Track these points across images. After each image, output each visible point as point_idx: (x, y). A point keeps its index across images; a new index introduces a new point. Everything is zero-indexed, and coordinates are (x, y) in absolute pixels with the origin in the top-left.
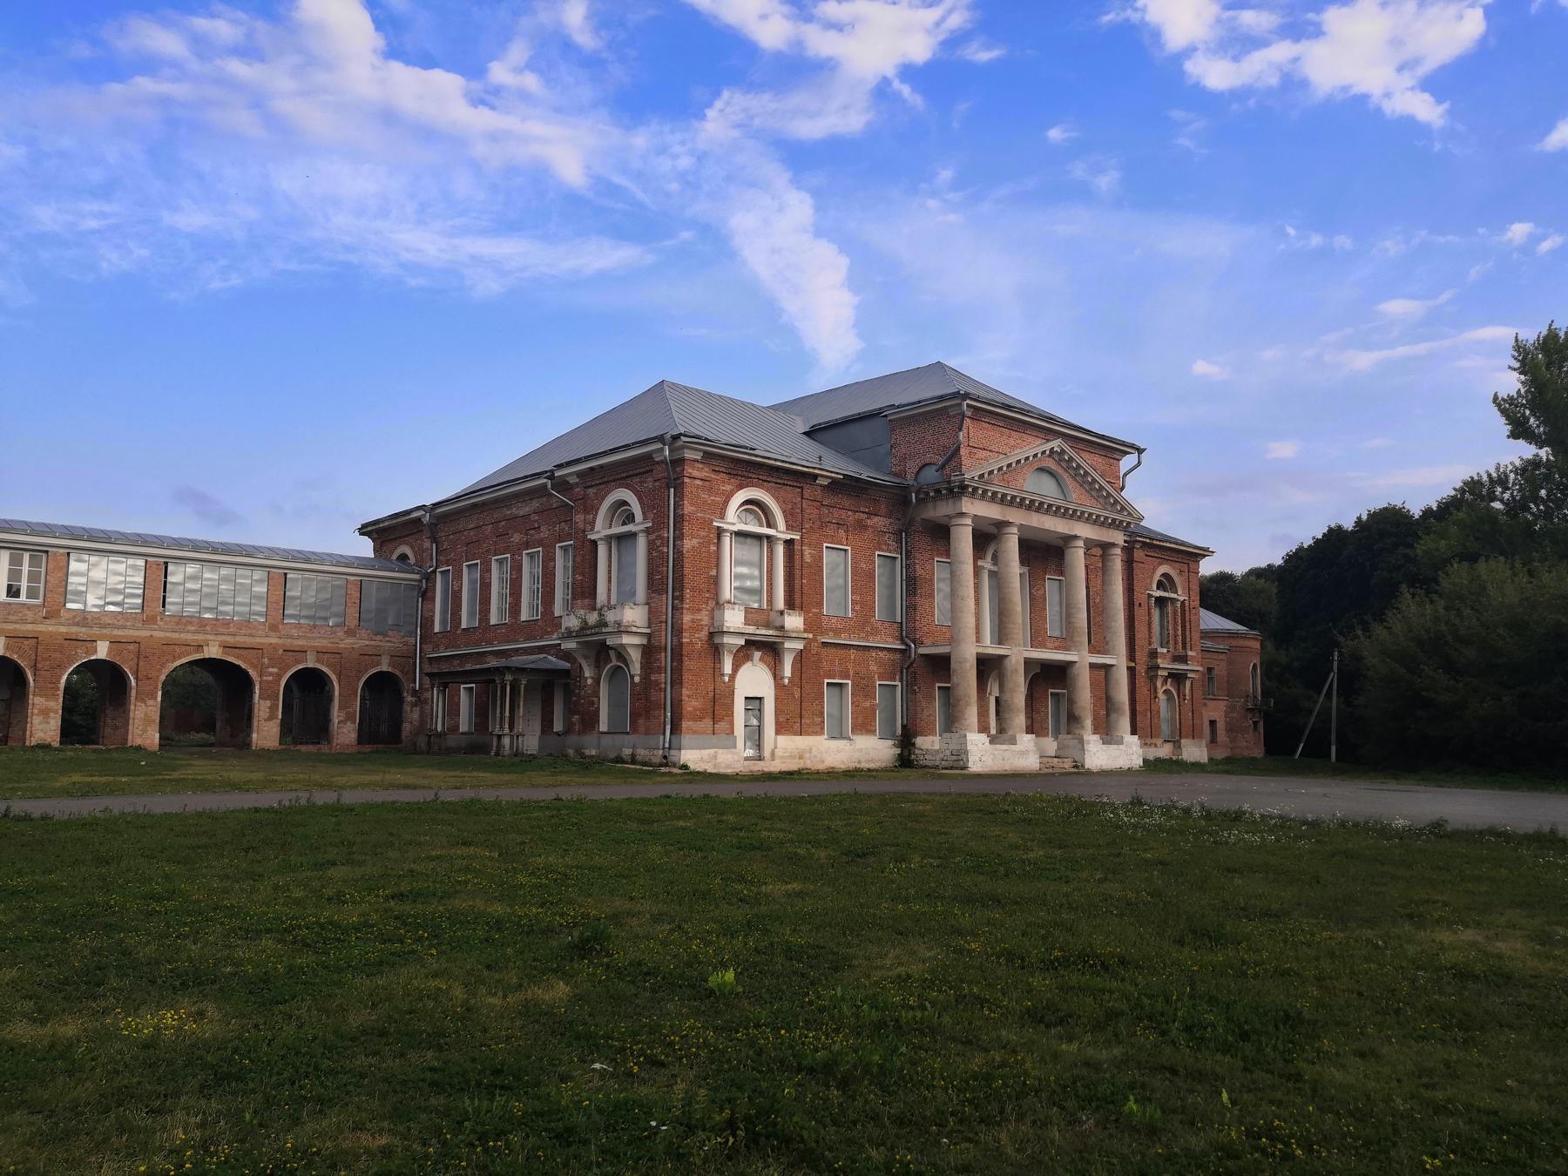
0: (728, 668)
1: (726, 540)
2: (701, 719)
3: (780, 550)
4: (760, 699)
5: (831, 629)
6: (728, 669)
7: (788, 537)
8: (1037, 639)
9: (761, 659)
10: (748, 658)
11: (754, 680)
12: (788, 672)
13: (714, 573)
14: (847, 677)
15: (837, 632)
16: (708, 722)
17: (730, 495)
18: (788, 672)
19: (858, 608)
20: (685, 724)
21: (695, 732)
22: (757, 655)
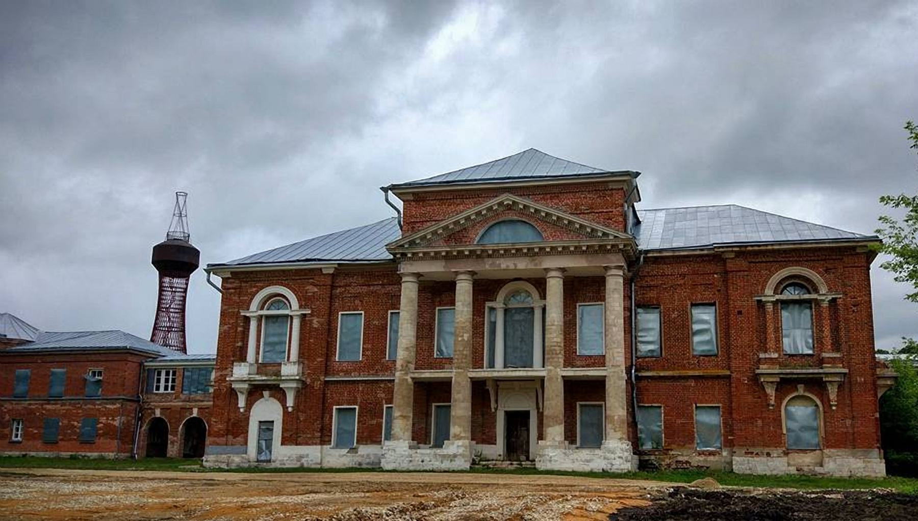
0: (242, 403)
2: (223, 436)
3: (296, 323)
4: (273, 422)
5: (342, 371)
6: (242, 403)
7: (299, 313)
8: (570, 360)
10: (262, 396)
11: (267, 410)
12: (290, 402)
13: (240, 344)
15: (347, 373)
16: (230, 437)
17: (253, 295)
18: (290, 402)
21: (218, 444)
22: (266, 393)
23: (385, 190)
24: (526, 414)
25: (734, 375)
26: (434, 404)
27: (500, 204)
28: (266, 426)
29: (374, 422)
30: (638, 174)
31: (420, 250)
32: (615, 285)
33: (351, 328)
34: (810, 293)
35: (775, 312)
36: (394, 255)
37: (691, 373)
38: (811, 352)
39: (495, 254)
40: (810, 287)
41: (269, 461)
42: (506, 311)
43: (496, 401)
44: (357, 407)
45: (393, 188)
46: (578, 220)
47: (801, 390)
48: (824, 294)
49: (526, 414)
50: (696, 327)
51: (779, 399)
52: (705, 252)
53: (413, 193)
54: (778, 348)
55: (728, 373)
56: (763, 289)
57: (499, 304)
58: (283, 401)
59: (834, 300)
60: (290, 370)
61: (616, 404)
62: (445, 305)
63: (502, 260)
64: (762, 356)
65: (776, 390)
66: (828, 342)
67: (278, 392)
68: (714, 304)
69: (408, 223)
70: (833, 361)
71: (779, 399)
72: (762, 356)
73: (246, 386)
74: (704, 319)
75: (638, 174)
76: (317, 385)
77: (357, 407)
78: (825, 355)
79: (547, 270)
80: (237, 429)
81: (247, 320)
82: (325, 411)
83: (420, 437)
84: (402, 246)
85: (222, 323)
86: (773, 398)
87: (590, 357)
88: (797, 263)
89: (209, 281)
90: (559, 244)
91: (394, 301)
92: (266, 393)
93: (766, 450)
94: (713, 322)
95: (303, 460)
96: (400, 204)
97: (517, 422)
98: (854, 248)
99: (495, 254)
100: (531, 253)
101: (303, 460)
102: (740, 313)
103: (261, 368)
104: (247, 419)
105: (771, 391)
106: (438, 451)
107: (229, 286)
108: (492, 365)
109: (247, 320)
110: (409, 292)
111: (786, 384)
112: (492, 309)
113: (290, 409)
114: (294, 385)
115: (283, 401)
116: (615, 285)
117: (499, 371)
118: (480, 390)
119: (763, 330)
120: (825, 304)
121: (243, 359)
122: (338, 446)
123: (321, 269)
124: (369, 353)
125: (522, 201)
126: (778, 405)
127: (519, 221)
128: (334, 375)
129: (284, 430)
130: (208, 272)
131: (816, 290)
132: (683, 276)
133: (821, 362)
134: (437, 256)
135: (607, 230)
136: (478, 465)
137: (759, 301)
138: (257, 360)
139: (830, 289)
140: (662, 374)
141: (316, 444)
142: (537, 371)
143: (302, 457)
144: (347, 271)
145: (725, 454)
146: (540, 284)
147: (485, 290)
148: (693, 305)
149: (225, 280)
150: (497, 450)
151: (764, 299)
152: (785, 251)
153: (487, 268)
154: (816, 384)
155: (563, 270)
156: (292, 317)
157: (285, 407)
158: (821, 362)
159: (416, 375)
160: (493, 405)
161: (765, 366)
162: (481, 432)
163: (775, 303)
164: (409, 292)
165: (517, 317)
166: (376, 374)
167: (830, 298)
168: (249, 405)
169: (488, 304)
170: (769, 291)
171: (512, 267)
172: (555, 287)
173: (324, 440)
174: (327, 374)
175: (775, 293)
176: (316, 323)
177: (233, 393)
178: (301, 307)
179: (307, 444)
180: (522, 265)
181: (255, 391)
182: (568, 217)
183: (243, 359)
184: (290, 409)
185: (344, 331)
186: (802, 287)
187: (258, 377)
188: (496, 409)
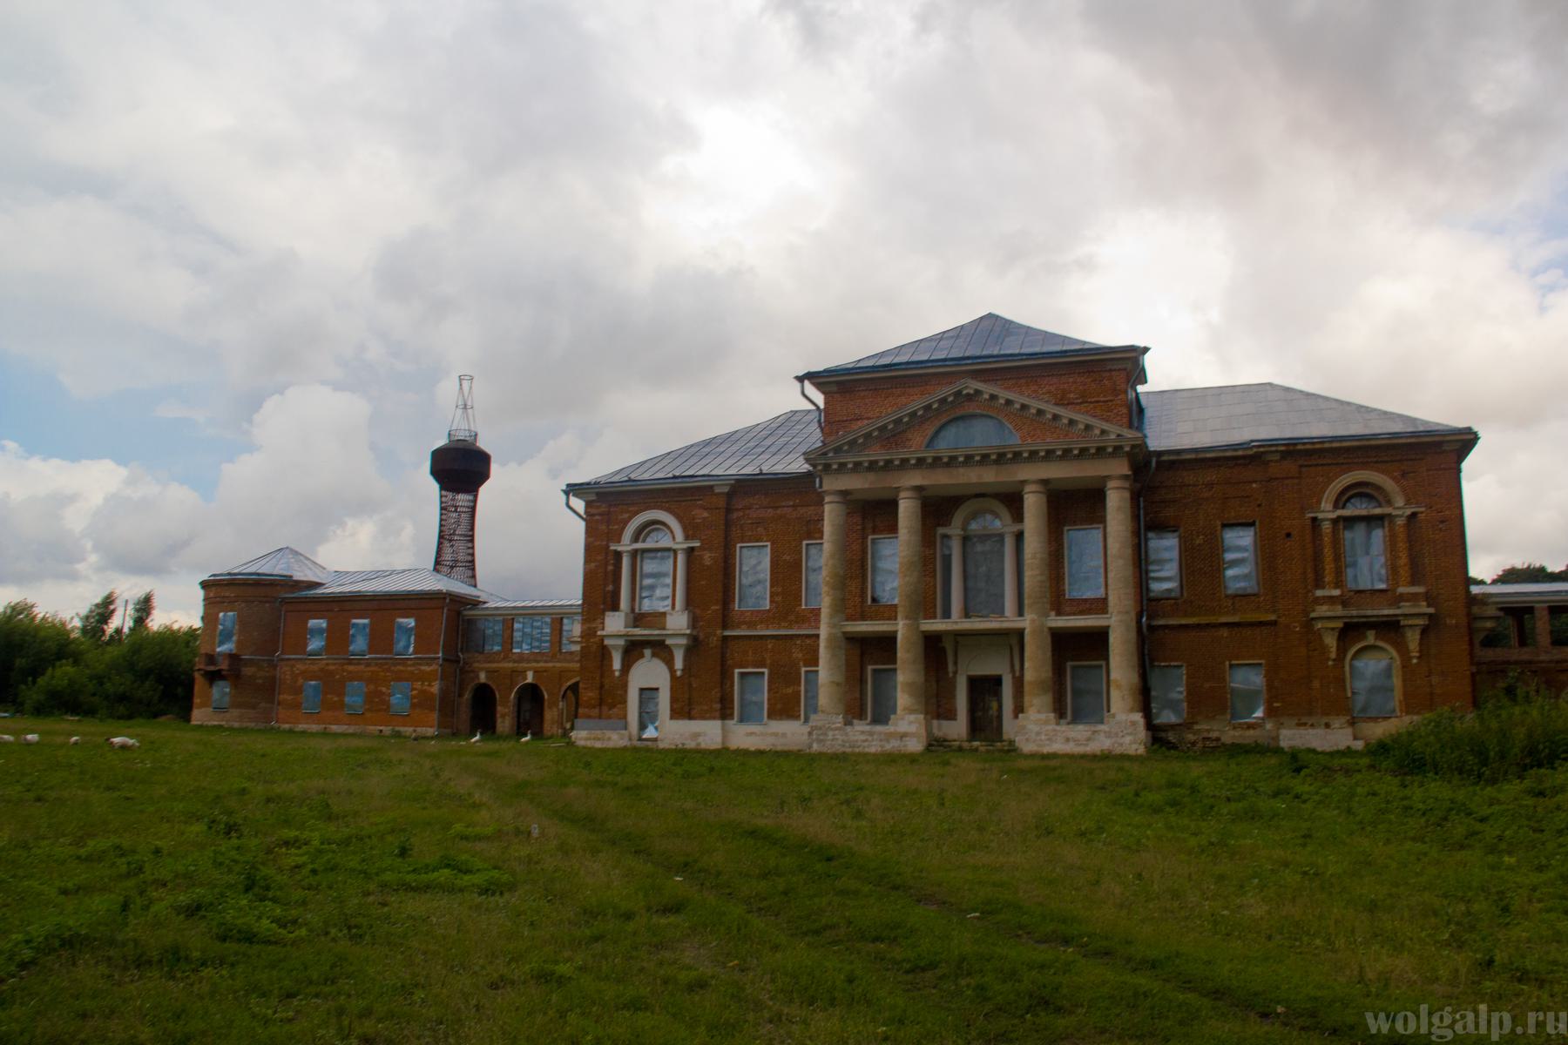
0: (617, 664)
1: (626, 562)
3: (681, 558)
6: (617, 664)
7: (685, 546)
8: (1059, 603)
9: (654, 655)
10: (642, 656)
11: (650, 673)
12: (679, 664)
13: (610, 588)
14: (763, 666)
15: (751, 625)
17: (626, 523)
19: (779, 599)
20: (581, 711)
21: (589, 717)
23: (800, 379)
24: (997, 681)
25: (1282, 620)
26: (870, 668)
27: (958, 394)
28: (648, 693)
29: (790, 690)
30: (1146, 350)
31: (850, 460)
32: (1116, 502)
33: (755, 565)
34: (1380, 506)
35: (1335, 531)
36: (814, 466)
37: (1223, 620)
38: (1383, 586)
39: (952, 462)
40: (1380, 498)
41: (655, 740)
42: (966, 539)
43: (956, 663)
44: (766, 671)
45: (811, 377)
46: (1066, 413)
47: (1371, 638)
48: (1400, 507)
49: (997, 681)
50: (1229, 556)
51: (1342, 651)
52: (1240, 453)
53: (838, 383)
54: (1338, 583)
55: (1273, 617)
56: (1319, 502)
57: (954, 530)
58: (669, 662)
59: (1414, 515)
60: (678, 622)
61: (1120, 666)
62: (881, 532)
63: (961, 470)
64: (1319, 593)
65: (1339, 639)
66: (1404, 573)
67: (660, 649)
68: (1252, 524)
69: (830, 420)
70: (1413, 598)
71: (1342, 651)
72: (1319, 593)
73: (621, 642)
74: (1240, 542)
75: (1146, 350)
76: (714, 641)
77: (766, 671)
78: (1401, 590)
79: (1023, 482)
80: (609, 699)
81: (618, 555)
82: (725, 675)
83: (855, 710)
84: (825, 454)
85: (588, 560)
86: (1334, 649)
87: (1086, 600)
88: (1365, 465)
89: (568, 505)
90: (1042, 448)
91: (813, 530)
92: (647, 652)
93: (1325, 720)
94: (1251, 548)
95: (700, 740)
96: (819, 398)
97: (985, 688)
98: (1440, 444)
99: (952, 462)
100: (1001, 459)
101: (700, 740)
102: (1288, 535)
103: (638, 619)
104: (624, 686)
105: (1331, 641)
106: (879, 728)
107: (593, 511)
108: (947, 614)
109: (618, 555)
110: (831, 515)
111: (1350, 631)
112: (946, 537)
113: (679, 673)
114: (684, 641)
115: (669, 662)
116: (1116, 502)
117: (958, 622)
118: (935, 649)
119: (1317, 558)
120: (1400, 522)
121: (615, 607)
122: (741, 720)
123: (711, 487)
124: (779, 599)
125: (987, 389)
126: (1340, 658)
127: (982, 416)
128: (733, 628)
129: (673, 700)
130: (567, 493)
131: (1389, 503)
132: (1210, 485)
133: (1399, 600)
134: (872, 466)
135: (1106, 426)
136: (936, 745)
137: (1314, 519)
138: (633, 610)
139: (1408, 502)
140: (1184, 621)
141: (714, 718)
142: (1009, 620)
143: (699, 735)
144: (745, 487)
145: (1269, 726)
146: (1013, 501)
147: (937, 509)
148: (1224, 526)
149: (588, 505)
150: (957, 728)
151: (1320, 516)
152: (1348, 449)
153: (940, 479)
154: (1390, 628)
155: (1045, 482)
156: (675, 551)
157: (672, 671)
158: (1399, 600)
159: (849, 629)
160: (951, 668)
161: (1325, 608)
162: (937, 704)
163: (1335, 521)
164: (831, 515)
165: (979, 548)
166: (790, 627)
167: (1408, 512)
168: (626, 668)
169: (941, 531)
170: (1326, 505)
171: (974, 480)
172: (1033, 503)
173: (725, 713)
174: (725, 627)
175: (1336, 506)
176: (708, 558)
177: (604, 653)
178: (687, 538)
179: (703, 718)
180: (988, 476)
181: (633, 650)
182: (1051, 409)
183: (615, 607)
184: (679, 673)
185: (745, 569)
186: (1370, 497)
187: (638, 631)
188: (955, 673)
